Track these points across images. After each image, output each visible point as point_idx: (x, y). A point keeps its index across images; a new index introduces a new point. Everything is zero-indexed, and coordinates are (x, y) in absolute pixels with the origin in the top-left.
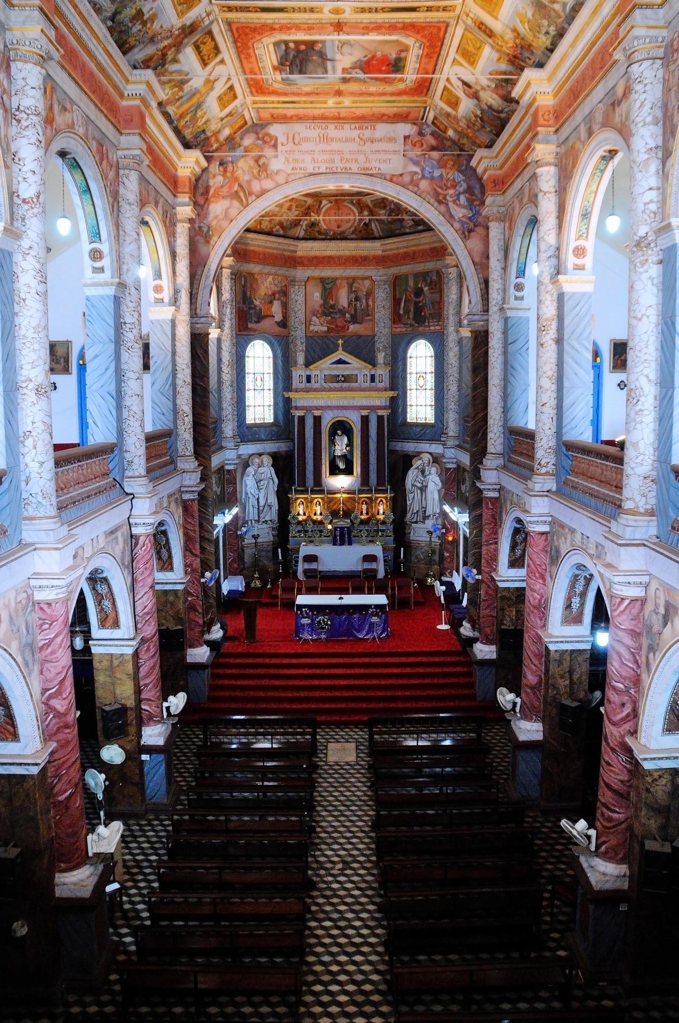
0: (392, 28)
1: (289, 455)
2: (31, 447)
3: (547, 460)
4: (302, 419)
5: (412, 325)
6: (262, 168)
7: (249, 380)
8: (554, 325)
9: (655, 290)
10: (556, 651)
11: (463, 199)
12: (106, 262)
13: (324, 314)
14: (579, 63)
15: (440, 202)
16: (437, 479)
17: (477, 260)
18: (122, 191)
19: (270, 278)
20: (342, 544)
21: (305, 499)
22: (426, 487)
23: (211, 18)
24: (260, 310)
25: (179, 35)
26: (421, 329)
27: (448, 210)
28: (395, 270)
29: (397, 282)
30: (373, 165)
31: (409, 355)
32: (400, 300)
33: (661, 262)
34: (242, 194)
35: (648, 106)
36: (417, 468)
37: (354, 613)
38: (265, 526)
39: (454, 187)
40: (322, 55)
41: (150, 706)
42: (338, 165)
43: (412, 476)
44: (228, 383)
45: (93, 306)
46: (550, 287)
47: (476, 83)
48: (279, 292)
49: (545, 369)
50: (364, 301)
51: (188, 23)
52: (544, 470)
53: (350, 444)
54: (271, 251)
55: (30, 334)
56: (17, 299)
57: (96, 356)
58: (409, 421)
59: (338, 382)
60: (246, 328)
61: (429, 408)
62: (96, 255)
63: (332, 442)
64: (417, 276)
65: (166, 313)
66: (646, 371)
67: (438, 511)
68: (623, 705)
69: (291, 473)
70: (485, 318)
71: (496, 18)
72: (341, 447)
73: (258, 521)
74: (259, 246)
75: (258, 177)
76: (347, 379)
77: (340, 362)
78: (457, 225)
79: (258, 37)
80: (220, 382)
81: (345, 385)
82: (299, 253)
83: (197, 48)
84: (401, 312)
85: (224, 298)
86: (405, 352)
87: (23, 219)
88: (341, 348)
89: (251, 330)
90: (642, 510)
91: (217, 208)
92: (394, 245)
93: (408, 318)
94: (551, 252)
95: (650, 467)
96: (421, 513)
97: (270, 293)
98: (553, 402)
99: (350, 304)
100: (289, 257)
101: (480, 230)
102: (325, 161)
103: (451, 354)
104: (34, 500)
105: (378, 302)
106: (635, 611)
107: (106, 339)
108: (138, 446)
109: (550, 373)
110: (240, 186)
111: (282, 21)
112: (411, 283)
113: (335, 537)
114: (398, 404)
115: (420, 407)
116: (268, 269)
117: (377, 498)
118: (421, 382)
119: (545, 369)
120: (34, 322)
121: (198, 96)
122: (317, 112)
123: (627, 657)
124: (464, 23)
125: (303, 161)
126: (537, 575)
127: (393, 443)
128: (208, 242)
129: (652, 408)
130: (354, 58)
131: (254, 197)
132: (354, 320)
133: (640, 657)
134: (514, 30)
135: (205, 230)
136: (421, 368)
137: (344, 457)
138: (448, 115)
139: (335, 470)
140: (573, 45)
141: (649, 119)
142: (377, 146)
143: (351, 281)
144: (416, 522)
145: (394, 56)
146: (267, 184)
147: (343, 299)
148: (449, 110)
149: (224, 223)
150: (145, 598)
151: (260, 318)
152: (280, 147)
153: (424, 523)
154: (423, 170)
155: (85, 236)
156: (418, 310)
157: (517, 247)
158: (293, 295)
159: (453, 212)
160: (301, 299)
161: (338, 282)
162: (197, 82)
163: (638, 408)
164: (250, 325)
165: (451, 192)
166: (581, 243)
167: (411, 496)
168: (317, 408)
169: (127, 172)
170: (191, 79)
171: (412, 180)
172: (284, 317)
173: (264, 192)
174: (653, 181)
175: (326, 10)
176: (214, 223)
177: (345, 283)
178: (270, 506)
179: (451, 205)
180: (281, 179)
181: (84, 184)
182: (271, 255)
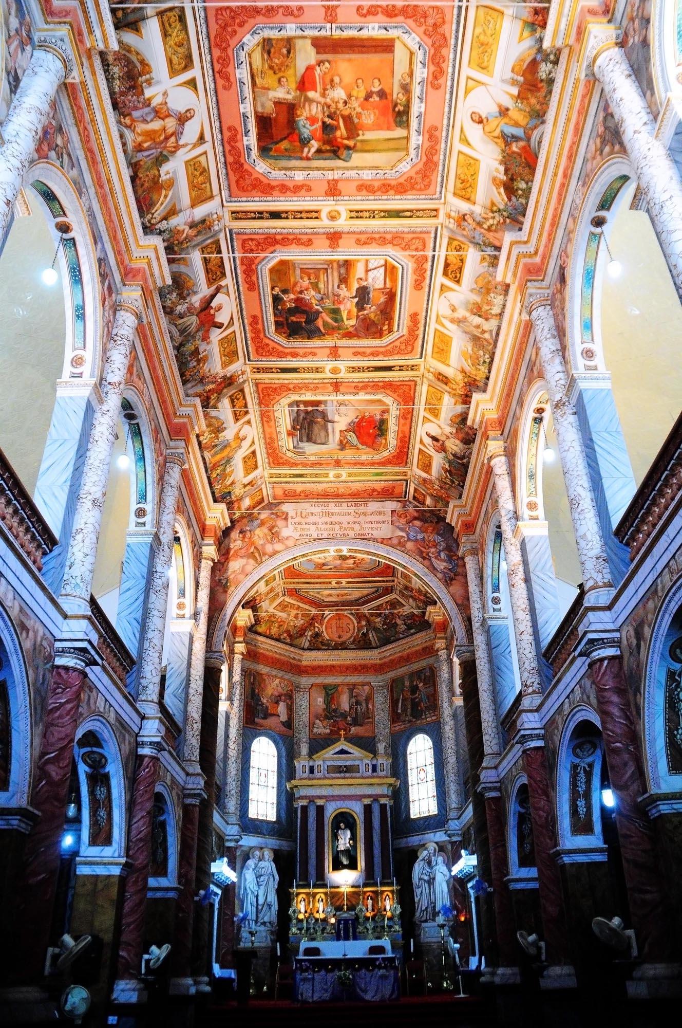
0: (375, 387)
1: (291, 855)
2: (80, 540)
3: (533, 680)
4: (304, 809)
5: (410, 721)
6: (274, 535)
7: (253, 774)
8: (521, 569)
9: (575, 430)
10: (572, 864)
11: (443, 555)
12: (148, 519)
13: (327, 717)
14: (508, 370)
15: (424, 558)
17: (460, 602)
18: (166, 477)
19: (277, 681)
20: (347, 938)
21: (308, 894)
22: (434, 879)
23: (245, 377)
24: (267, 708)
25: (220, 384)
27: (432, 564)
28: (392, 674)
29: (394, 686)
30: (367, 532)
32: (398, 700)
33: (575, 413)
34: (257, 555)
35: (546, 330)
36: (423, 859)
37: (359, 969)
39: (435, 546)
40: (324, 415)
41: (128, 952)
42: (337, 530)
43: (418, 869)
44: (233, 759)
45: (132, 551)
46: (513, 540)
47: (443, 434)
48: (285, 695)
49: (518, 604)
51: (228, 375)
52: (530, 690)
53: (354, 838)
54: (278, 656)
55: (96, 463)
56: (91, 440)
57: (129, 589)
58: (412, 817)
59: (340, 772)
60: (253, 722)
61: (431, 800)
62: (141, 513)
63: (335, 837)
64: (412, 675)
65: (187, 626)
66: (580, 483)
68: (626, 764)
70: (471, 648)
71: (448, 365)
72: (344, 841)
74: (267, 650)
75: (271, 542)
76: (348, 769)
77: (343, 752)
78: (440, 575)
79: (278, 398)
80: (226, 758)
81: (347, 775)
82: (304, 663)
83: (232, 401)
84: (399, 711)
85: (234, 680)
86: (405, 750)
87: (107, 394)
88: (342, 739)
89: (257, 724)
90: (601, 584)
91: (235, 565)
92: (391, 651)
93: (406, 715)
94: (511, 515)
95: (600, 550)
96: (430, 909)
97: (277, 694)
98: (530, 630)
99: (351, 708)
100: (296, 666)
101: (460, 578)
102: (327, 530)
103: (447, 728)
104: (73, 581)
105: (377, 705)
106: (615, 670)
107: (140, 576)
108: (154, 674)
109: (524, 606)
110: (256, 548)
111: (296, 381)
112: (407, 683)
114: (400, 795)
115: (422, 801)
116: (274, 672)
117: (383, 892)
118: (422, 775)
119: (518, 604)
120: (101, 457)
121: (228, 449)
122: (320, 488)
123: (618, 714)
124: (428, 379)
125: (309, 530)
126: (540, 792)
127: (398, 841)
128: (226, 592)
129: (590, 507)
130: (348, 420)
131: (267, 557)
132: (355, 722)
133: (631, 712)
134: (463, 371)
135: (224, 582)
136: (421, 763)
137: (346, 852)
138: (425, 481)
139: (337, 866)
140: (501, 359)
141: (549, 336)
142: (369, 518)
143: (352, 687)
145: (378, 417)
146: (278, 547)
147: (345, 703)
148: (424, 475)
149: (241, 577)
150: (141, 823)
151: (266, 716)
152: (290, 520)
153: (434, 920)
154: (408, 535)
155: (134, 498)
156: (415, 705)
157: (490, 564)
158: (298, 700)
159: (436, 566)
160: (305, 704)
161: (340, 688)
162: (228, 435)
163: (579, 510)
164: (256, 720)
165: (433, 550)
166: (533, 499)
167: (418, 891)
168: (320, 797)
169: (172, 465)
170: (225, 428)
171: (400, 542)
173: (276, 553)
174: (560, 368)
175: (327, 370)
176: (231, 577)
177: (346, 689)
179: (433, 559)
180: (290, 543)
181: (141, 453)
182: (278, 660)
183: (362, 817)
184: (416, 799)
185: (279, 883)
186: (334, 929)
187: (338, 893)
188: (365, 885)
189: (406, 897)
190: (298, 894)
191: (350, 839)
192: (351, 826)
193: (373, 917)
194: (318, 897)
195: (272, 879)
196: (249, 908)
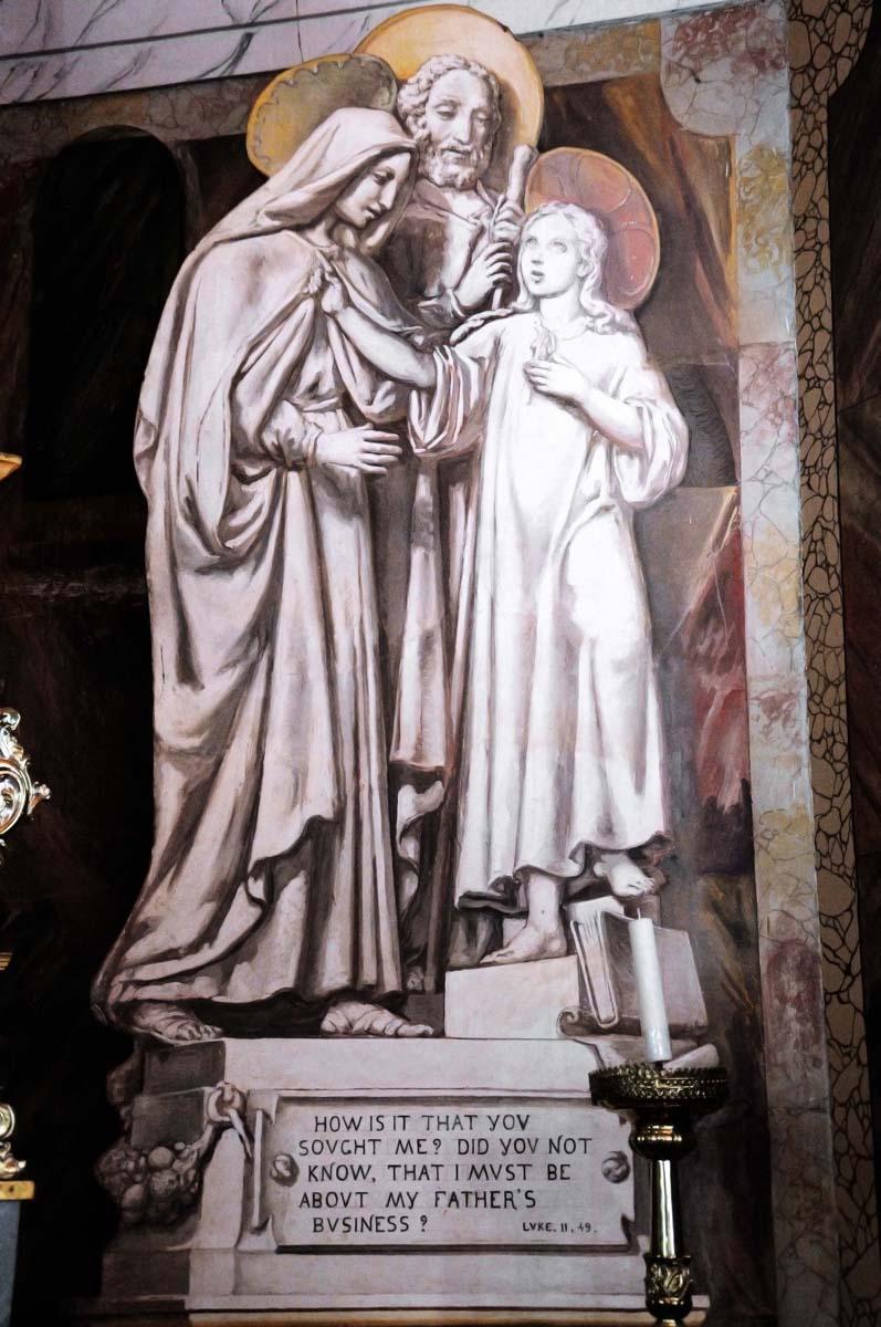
22: (458, 469)
36: (325, 212)
43: (231, 322)
67: (643, 816)
144: (295, 1014)
153: (418, 1007)
167: (219, 608)
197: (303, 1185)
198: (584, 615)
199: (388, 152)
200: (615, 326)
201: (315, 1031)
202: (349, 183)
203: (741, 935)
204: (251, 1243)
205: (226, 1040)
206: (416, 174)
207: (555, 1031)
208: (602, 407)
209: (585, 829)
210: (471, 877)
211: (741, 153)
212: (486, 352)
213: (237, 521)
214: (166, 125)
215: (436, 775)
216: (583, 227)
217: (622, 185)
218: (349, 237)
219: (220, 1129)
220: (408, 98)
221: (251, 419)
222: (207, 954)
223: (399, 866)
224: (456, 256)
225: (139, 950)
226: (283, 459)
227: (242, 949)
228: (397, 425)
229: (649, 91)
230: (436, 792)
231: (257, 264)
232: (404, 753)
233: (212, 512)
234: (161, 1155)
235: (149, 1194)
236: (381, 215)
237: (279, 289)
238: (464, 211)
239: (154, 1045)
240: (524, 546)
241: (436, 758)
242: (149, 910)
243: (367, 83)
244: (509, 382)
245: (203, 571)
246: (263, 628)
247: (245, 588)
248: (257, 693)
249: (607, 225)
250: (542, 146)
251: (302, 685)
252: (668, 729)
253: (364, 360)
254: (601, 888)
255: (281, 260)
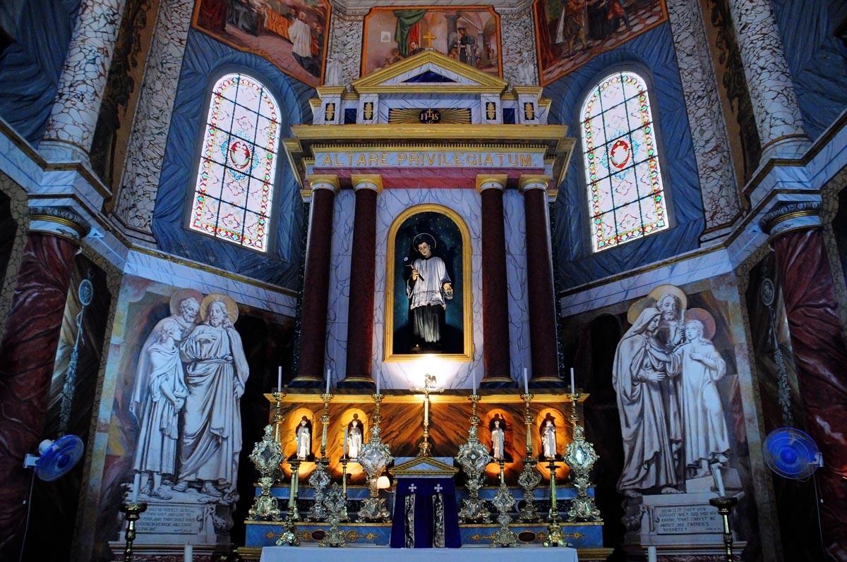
4: (326, 199)
16: (709, 352)
20: (425, 541)
21: (316, 408)
22: (678, 378)
26: (608, 44)
31: (582, 119)
32: (555, 23)
36: (645, 330)
38: (193, 496)
43: (629, 355)
48: (308, 11)
50: (481, 44)
53: (454, 276)
59: (424, 122)
60: (222, 30)
63: (404, 276)
67: (725, 445)
69: (288, 346)
72: (430, 284)
73: (173, 479)
77: (428, 77)
84: (560, 40)
89: (230, 36)
105: (509, 44)
113: (399, 517)
115: (625, 202)
117: (536, 408)
136: (616, 127)
137: (433, 312)
139: (407, 343)
144: (656, 490)
151: (256, 27)
153: (680, 487)
158: (338, 33)
160: (354, 41)
161: (429, 15)
164: (229, 28)
167: (632, 412)
168: (363, 170)
172: (314, 56)
177: (441, 17)
178: (218, 440)
183: (477, 226)
184: (605, 205)
185: (249, 384)
186: (387, 506)
187: (410, 407)
188: (485, 388)
189: (601, 420)
190: (288, 409)
191: (444, 282)
192: (451, 256)
193: (512, 477)
194: (348, 417)
195: (229, 370)
196: (156, 451)
197: (661, 523)
198: (707, 405)
199: (656, 316)
200: (708, 343)
201: (661, 494)
202: (648, 323)
203: (748, 468)
204: (651, 533)
205: (644, 496)
206: (662, 319)
207: (709, 491)
208: (707, 361)
209: (712, 449)
210: (689, 461)
211: (730, 304)
212: (681, 353)
213: (634, 394)
214: (614, 312)
215: (680, 441)
216: (699, 324)
217: (705, 314)
218: (650, 334)
219: (643, 513)
220: (659, 304)
221: (634, 373)
222: (637, 480)
223: (674, 460)
224: (672, 334)
225: (624, 480)
226: (642, 380)
227: (644, 478)
228: (664, 370)
229: (709, 293)
230: (680, 444)
231: (632, 342)
232: (673, 437)
233: (629, 393)
234: (633, 518)
235: (631, 525)
236: (656, 328)
237: (637, 347)
238: (673, 324)
239: (631, 498)
240: (693, 392)
241: (679, 438)
242: (625, 471)
243: (651, 303)
244: (686, 358)
245: (629, 405)
246: (641, 415)
247: (637, 407)
248: (642, 428)
249: (703, 322)
250: (688, 308)
251: (650, 426)
252: (728, 426)
253: (656, 358)
254: (717, 461)
255: (637, 340)
